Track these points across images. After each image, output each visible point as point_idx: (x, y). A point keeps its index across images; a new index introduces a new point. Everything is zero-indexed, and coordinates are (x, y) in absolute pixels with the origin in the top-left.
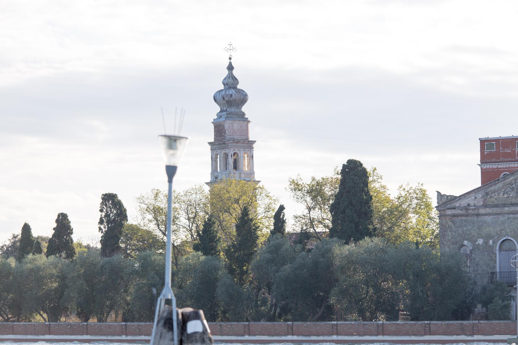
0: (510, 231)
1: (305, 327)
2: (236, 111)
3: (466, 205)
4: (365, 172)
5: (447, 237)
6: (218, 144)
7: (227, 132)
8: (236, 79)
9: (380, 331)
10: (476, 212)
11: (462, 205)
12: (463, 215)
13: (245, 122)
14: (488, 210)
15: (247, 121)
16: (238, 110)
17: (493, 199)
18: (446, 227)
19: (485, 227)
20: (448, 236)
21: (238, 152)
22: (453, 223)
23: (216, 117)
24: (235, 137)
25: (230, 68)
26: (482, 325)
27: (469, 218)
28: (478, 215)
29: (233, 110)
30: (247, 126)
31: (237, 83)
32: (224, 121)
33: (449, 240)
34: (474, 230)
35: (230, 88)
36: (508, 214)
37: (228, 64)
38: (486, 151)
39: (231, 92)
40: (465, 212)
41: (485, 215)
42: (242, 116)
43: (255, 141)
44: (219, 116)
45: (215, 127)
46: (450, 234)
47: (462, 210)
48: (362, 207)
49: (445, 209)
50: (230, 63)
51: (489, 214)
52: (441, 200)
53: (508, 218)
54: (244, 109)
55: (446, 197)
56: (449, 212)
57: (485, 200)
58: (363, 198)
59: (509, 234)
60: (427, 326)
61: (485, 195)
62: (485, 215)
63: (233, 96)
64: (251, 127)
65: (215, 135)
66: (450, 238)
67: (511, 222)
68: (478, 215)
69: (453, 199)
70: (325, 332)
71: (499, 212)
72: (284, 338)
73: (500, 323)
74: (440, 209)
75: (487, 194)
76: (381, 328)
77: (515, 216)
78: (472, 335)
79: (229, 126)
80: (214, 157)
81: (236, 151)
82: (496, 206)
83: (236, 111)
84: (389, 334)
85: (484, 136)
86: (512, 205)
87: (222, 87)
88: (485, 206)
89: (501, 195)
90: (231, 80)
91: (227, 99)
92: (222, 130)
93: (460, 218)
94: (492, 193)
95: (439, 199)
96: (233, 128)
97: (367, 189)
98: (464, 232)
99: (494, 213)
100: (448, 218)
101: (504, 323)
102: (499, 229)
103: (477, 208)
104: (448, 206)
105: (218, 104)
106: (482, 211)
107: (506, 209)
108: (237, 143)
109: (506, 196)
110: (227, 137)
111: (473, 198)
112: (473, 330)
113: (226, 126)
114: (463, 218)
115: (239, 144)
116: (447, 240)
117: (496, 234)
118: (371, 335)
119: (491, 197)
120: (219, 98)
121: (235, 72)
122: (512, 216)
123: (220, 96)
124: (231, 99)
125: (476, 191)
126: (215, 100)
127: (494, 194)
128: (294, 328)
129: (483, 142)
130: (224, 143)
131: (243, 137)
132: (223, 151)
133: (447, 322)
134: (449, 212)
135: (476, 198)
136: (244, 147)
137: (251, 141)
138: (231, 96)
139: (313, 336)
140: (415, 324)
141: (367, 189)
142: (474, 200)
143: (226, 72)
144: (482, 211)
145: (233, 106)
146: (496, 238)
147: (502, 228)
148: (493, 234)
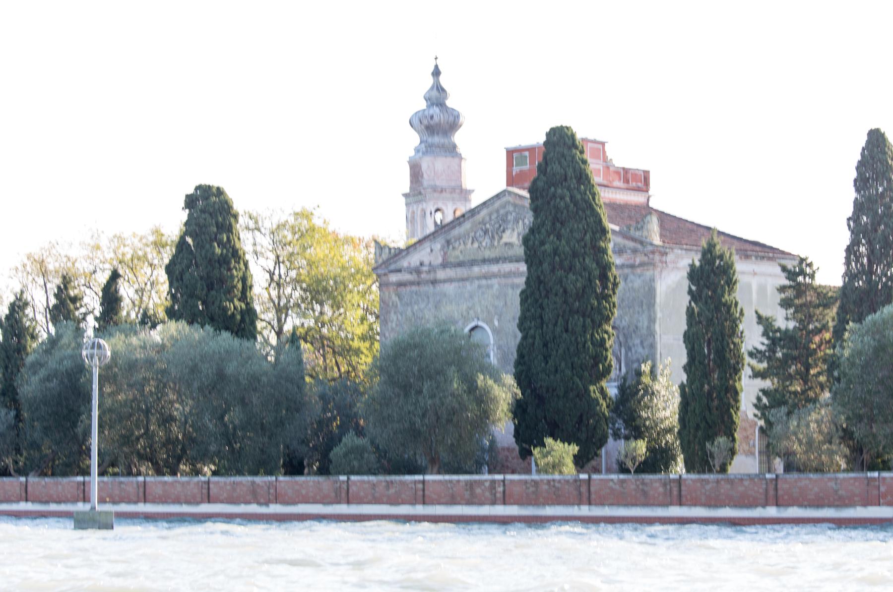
0: (482, 311)
1: (43, 486)
2: (442, 141)
3: (418, 263)
4: (226, 206)
5: (390, 324)
6: (414, 196)
7: (425, 176)
8: (443, 90)
9: (141, 494)
10: (431, 276)
11: (413, 265)
12: (412, 283)
13: (456, 160)
14: (450, 273)
15: (460, 158)
16: (446, 141)
17: (457, 253)
18: (388, 305)
19: (444, 303)
20: (392, 322)
21: (444, 208)
22: (399, 297)
23: (412, 153)
24: (438, 183)
25: (436, 73)
26: (283, 485)
27: (423, 289)
28: (434, 282)
29: (437, 139)
30: (460, 166)
31: (446, 97)
32: (420, 158)
33: (392, 329)
34: (430, 310)
35: (432, 104)
36: (478, 278)
37: (432, 69)
38: (516, 170)
39: (431, 112)
40: (416, 276)
41: (445, 281)
42: (452, 150)
43: (473, 191)
44: (417, 150)
45: (411, 169)
46: (395, 319)
47: (411, 273)
48: (213, 269)
49: (387, 271)
50: (436, 67)
51: (450, 280)
52: (380, 255)
53: (479, 287)
54: (459, 138)
55: (387, 250)
56: (394, 278)
57: (445, 254)
58: (213, 253)
59: (480, 317)
60: (204, 485)
61: (446, 245)
62: (445, 281)
63: (435, 117)
64: (467, 168)
65: (412, 182)
66: (394, 325)
67: (483, 293)
68: (434, 282)
69: (398, 254)
70: (69, 496)
71: (465, 275)
72: (14, 507)
73: (307, 482)
74: (380, 271)
75: (448, 242)
76: (142, 490)
77: (489, 282)
78: (267, 504)
79: (429, 167)
80: (409, 216)
81: (440, 205)
82: (460, 264)
83: (442, 141)
84: (154, 501)
85: (513, 144)
86: (485, 261)
87: (423, 105)
88: (444, 265)
89: (469, 245)
90: (435, 93)
91: (425, 122)
92: (419, 173)
93: (408, 289)
94: (455, 241)
95: (378, 253)
96: (434, 169)
97: (228, 238)
98: (414, 314)
99: (459, 276)
100: (391, 289)
101: (314, 482)
102: (465, 307)
103: (432, 269)
104: (393, 267)
105: (415, 130)
106: (441, 274)
107: (476, 270)
108: (442, 191)
109: (476, 245)
110: (425, 183)
111: (429, 250)
112: (269, 494)
113: (424, 166)
114: (414, 288)
115: (444, 194)
116: (390, 328)
117: (460, 316)
118: (129, 501)
119: (454, 248)
120: (416, 122)
121: (443, 81)
122: (484, 282)
123: (417, 119)
124: (432, 123)
125: (431, 237)
126: (412, 126)
127: (458, 243)
128: (29, 489)
129: (510, 153)
130: (420, 193)
131: (453, 184)
132: (420, 207)
133: (232, 479)
134: (394, 278)
135: (432, 250)
136: (453, 200)
137: (466, 190)
138: (432, 117)
139: (52, 502)
140: (188, 483)
141: (228, 238)
142: (429, 254)
143: (430, 81)
144: (441, 274)
145: (438, 134)
146: (460, 323)
147: (470, 305)
148: (456, 317)
